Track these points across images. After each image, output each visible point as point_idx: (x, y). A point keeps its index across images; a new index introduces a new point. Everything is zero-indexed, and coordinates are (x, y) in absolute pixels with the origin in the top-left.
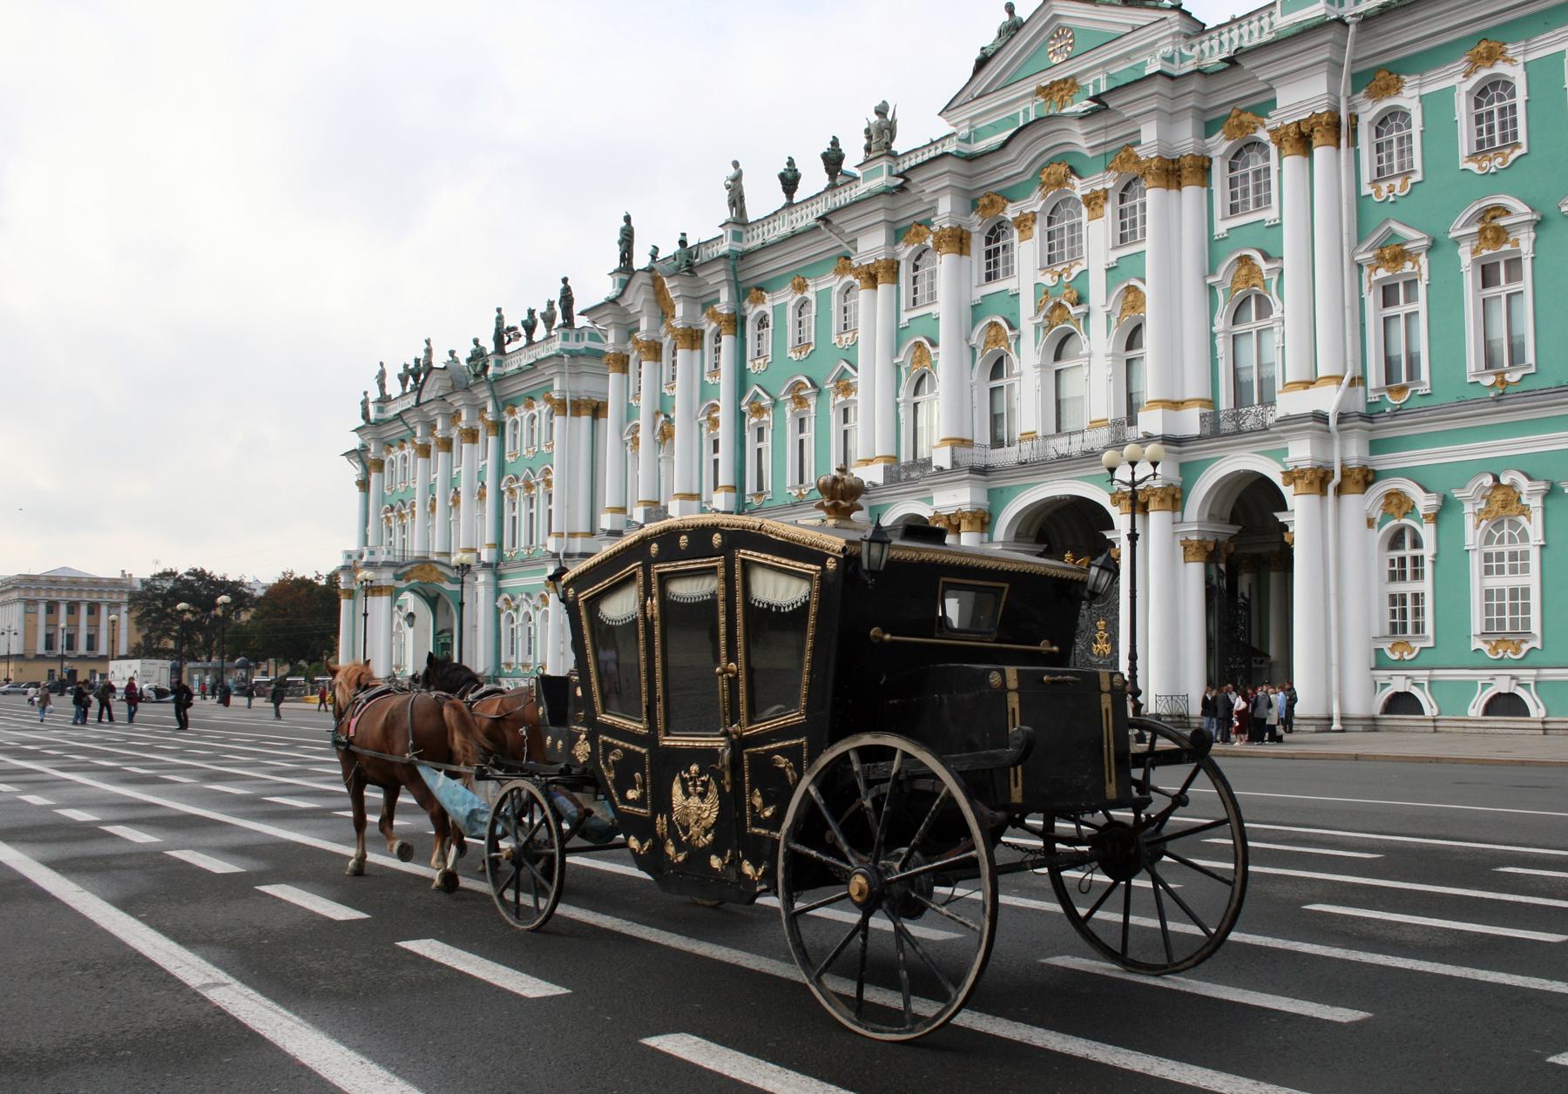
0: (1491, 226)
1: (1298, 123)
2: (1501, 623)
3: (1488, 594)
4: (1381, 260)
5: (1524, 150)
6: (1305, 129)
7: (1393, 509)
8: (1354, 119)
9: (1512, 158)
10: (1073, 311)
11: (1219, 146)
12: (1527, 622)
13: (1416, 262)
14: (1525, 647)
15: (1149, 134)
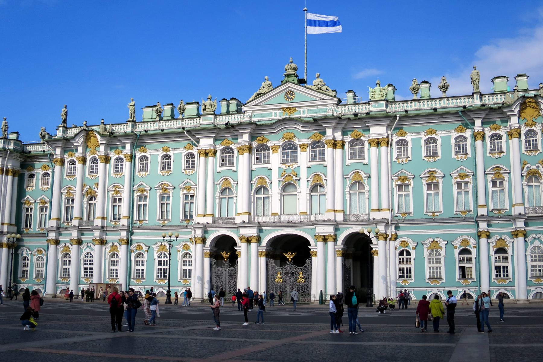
0: (432, 175)
1: (378, 139)
2: (433, 276)
3: (430, 268)
4: (399, 179)
5: (440, 158)
6: (379, 141)
7: (402, 245)
8: (392, 140)
9: (437, 159)
10: (294, 178)
11: (348, 139)
12: (440, 276)
13: (409, 181)
14: (440, 282)
15: (329, 131)
